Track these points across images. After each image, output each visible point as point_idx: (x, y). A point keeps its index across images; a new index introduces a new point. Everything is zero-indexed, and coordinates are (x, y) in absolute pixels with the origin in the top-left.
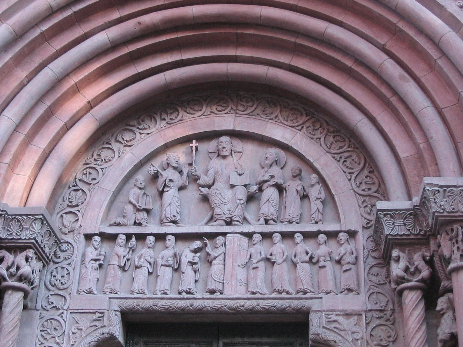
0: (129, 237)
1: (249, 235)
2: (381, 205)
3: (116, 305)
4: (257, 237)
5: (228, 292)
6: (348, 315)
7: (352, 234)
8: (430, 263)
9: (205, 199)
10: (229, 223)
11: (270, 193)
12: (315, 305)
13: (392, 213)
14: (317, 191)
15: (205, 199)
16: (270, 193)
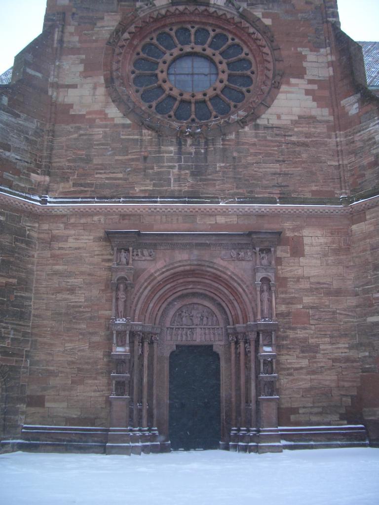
0: (176, 328)
1: (201, 328)
2: (228, 327)
3: (175, 343)
4: (202, 329)
5: (197, 341)
6: (221, 345)
7: (222, 328)
8: (237, 338)
9: (191, 319)
10: (197, 325)
11: (205, 319)
12: (214, 343)
13: (230, 328)
14: (215, 318)
15: (191, 319)
16: (205, 319)
